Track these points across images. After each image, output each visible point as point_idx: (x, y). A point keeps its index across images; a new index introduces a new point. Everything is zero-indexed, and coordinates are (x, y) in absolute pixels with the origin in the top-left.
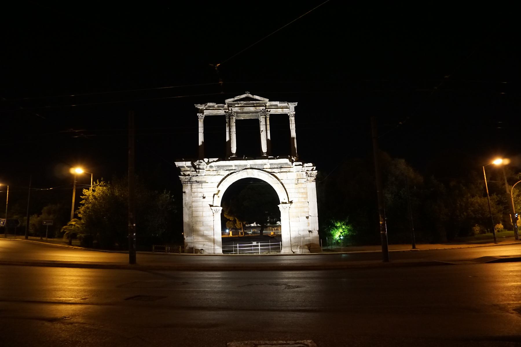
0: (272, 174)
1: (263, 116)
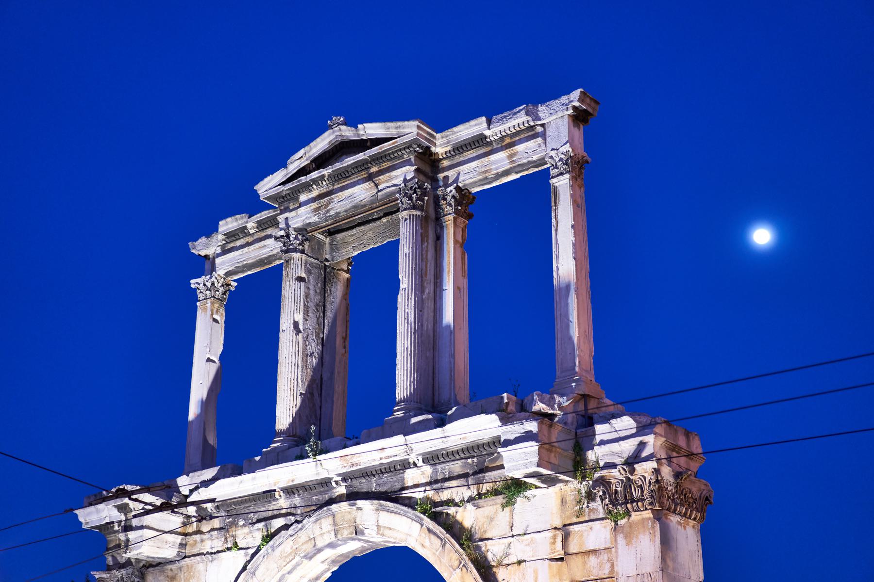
0: (436, 517)
1: (405, 213)
